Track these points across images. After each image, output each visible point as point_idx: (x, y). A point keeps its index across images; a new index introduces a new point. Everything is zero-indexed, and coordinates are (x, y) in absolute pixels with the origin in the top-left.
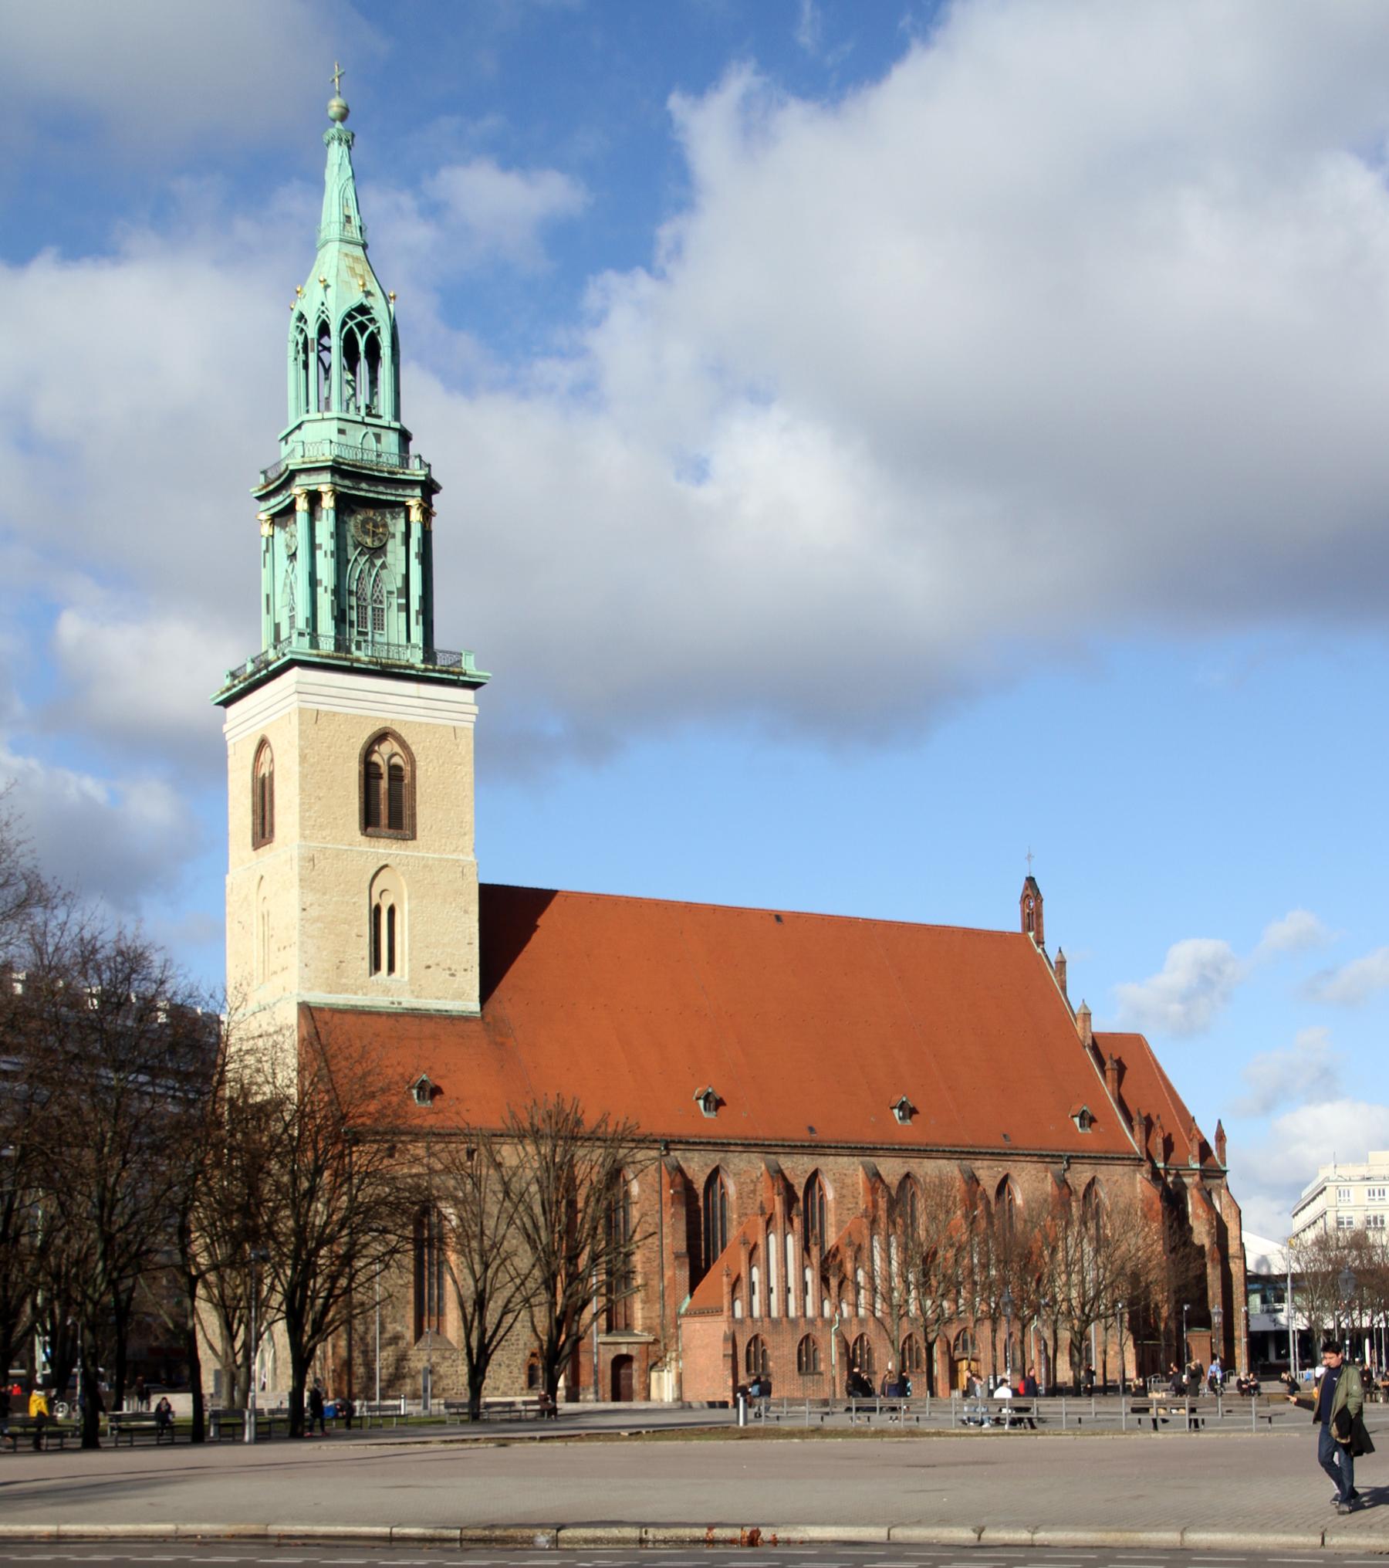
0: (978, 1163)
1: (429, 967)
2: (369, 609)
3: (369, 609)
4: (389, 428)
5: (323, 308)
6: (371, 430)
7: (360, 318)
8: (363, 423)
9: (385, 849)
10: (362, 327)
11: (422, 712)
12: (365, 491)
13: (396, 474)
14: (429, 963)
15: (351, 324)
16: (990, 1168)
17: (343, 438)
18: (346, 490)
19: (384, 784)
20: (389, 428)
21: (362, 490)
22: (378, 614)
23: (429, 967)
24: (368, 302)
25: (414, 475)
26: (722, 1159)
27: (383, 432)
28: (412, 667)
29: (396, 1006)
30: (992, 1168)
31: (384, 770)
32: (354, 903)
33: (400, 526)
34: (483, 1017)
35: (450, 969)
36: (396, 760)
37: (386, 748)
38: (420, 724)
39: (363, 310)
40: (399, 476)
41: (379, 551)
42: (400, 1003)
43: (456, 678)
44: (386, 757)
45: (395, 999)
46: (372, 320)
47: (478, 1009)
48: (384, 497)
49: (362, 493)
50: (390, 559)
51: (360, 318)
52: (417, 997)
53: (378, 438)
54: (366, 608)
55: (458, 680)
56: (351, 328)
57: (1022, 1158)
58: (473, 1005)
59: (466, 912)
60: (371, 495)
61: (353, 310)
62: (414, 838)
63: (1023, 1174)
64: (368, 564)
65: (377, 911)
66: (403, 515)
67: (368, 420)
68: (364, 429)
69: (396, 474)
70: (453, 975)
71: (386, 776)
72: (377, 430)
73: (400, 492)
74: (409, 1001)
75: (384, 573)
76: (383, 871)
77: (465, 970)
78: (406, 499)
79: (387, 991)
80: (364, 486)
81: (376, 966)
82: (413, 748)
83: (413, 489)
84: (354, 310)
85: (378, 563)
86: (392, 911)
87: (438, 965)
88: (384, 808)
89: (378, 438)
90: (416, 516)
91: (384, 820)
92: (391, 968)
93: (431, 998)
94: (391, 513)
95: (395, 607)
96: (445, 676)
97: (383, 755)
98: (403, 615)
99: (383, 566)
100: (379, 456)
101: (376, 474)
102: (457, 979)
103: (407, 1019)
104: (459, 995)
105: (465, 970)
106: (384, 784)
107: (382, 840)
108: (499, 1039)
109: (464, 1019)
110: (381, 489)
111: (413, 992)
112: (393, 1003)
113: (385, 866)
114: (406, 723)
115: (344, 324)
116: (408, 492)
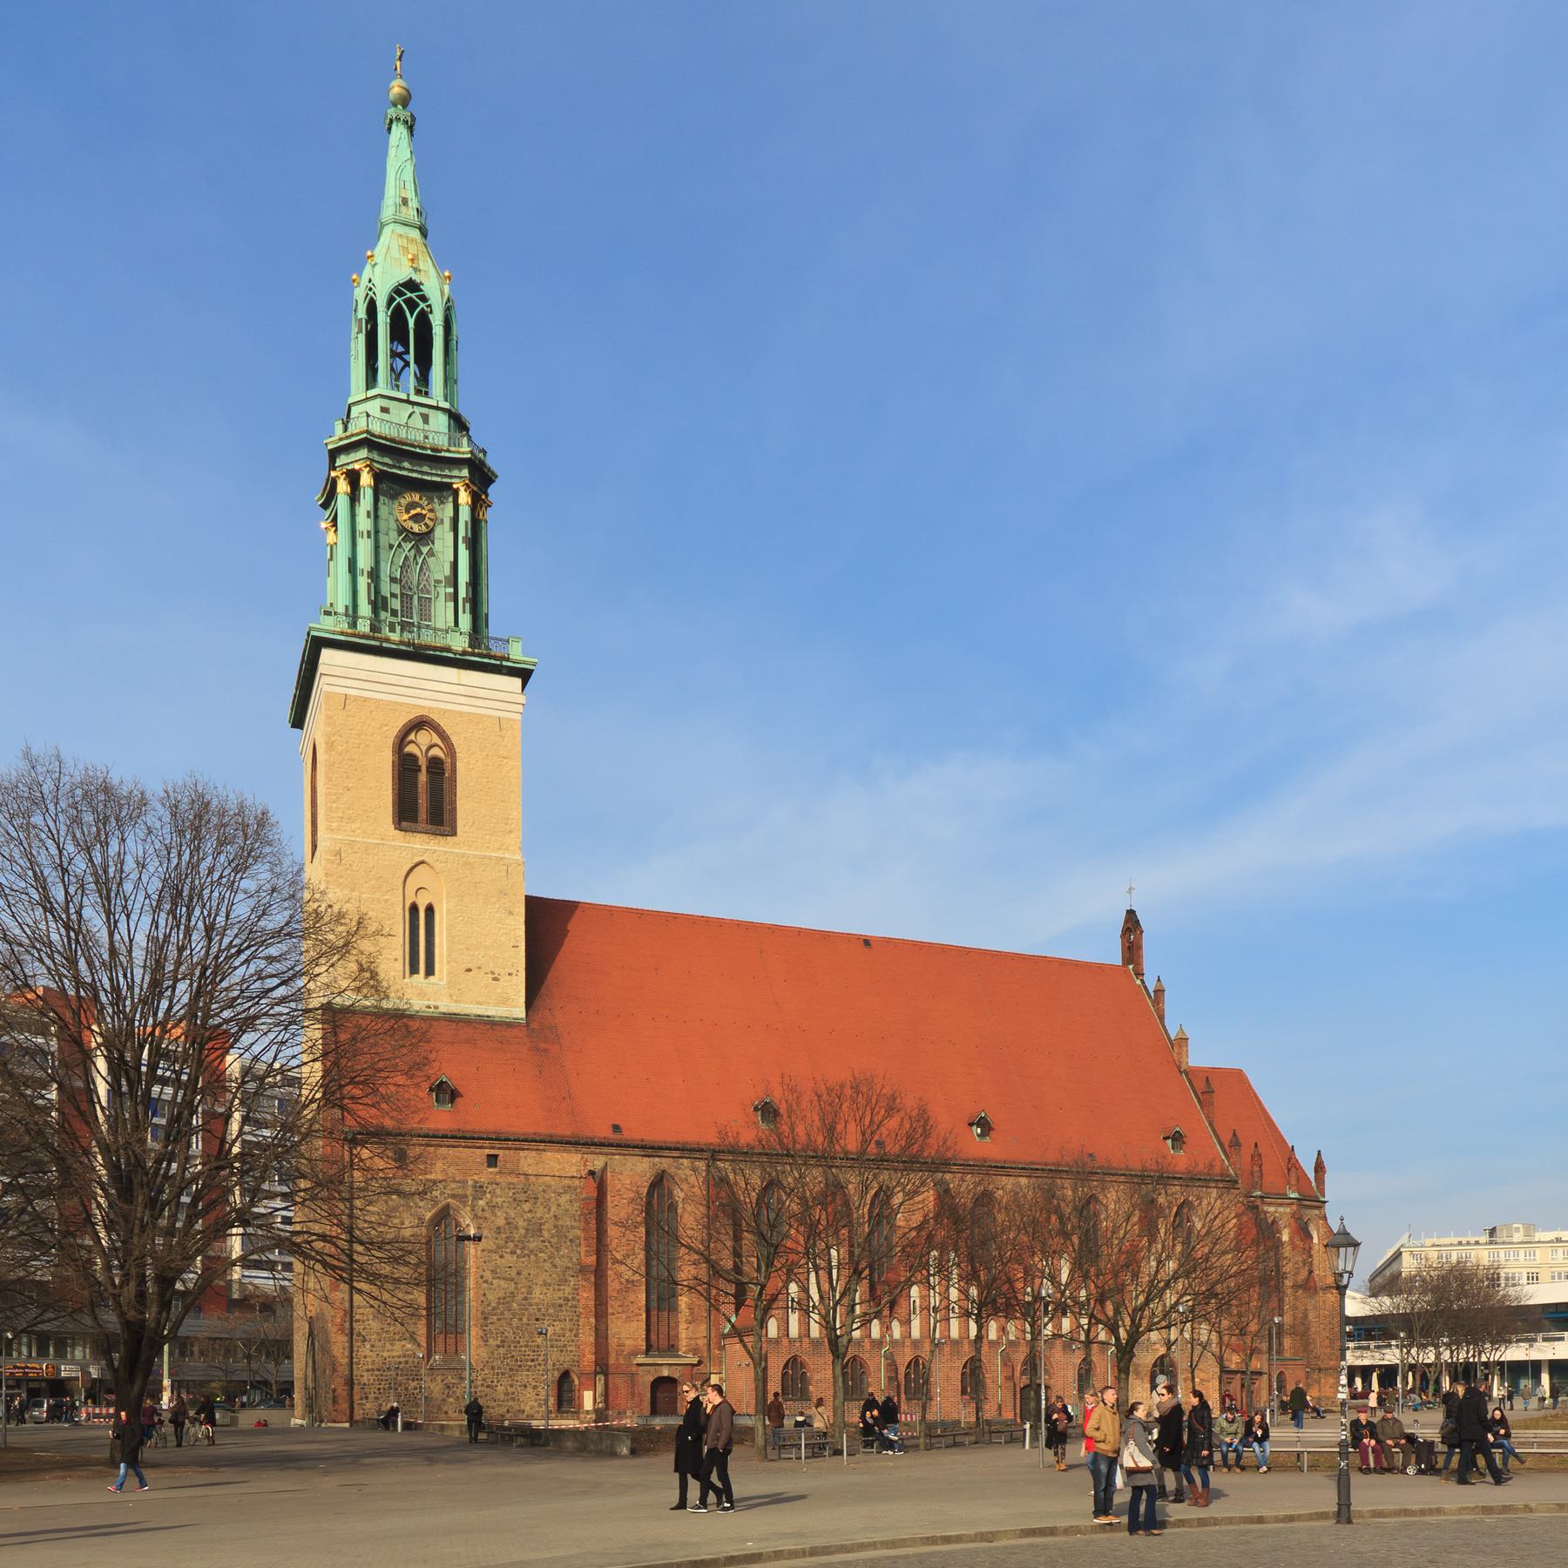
1: (469, 970)
2: (416, 597)
3: (416, 597)
4: (437, 408)
5: (370, 285)
6: (418, 410)
7: (409, 295)
8: (408, 402)
9: (420, 845)
10: (412, 305)
11: (462, 700)
12: (407, 470)
13: (440, 451)
14: (469, 966)
15: (399, 300)
17: (385, 416)
19: (423, 777)
20: (437, 408)
21: (404, 469)
22: (426, 604)
23: (469, 970)
24: (417, 278)
25: (459, 452)
27: (431, 412)
28: (448, 650)
29: (432, 1010)
31: (423, 763)
32: (386, 901)
33: (449, 509)
34: (528, 1024)
35: (493, 973)
36: (435, 752)
37: (424, 738)
38: (461, 714)
39: (412, 285)
40: (443, 454)
41: (426, 537)
42: (436, 1007)
43: (499, 663)
44: (424, 748)
45: (432, 1003)
46: (424, 299)
47: (523, 1015)
48: (429, 478)
49: (405, 473)
50: (438, 546)
51: (409, 295)
52: (456, 1001)
53: (425, 418)
54: (411, 597)
55: (501, 666)
56: (399, 303)
58: (519, 1012)
59: (511, 913)
60: (415, 475)
61: (400, 285)
62: (454, 833)
64: (413, 552)
65: (414, 909)
66: (451, 499)
67: (414, 398)
68: (410, 408)
69: (440, 451)
70: (495, 979)
71: (424, 768)
73: (447, 472)
74: (447, 1005)
75: (431, 560)
76: (422, 865)
77: (510, 974)
78: (453, 481)
79: (422, 994)
80: (406, 465)
81: (414, 970)
82: (454, 739)
83: (460, 470)
84: (403, 285)
85: (425, 550)
86: (430, 910)
87: (479, 968)
88: (423, 801)
89: (425, 418)
90: (464, 498)
91: (423, 814)
92: (430, 971)
93: (471, 1003)
94: (439, 499)
95: (442, 597)
96: (486, 660)
97: (421, 744)
98: (451, 604)
99: (431, 553)
100: (426, 437)
101: (418, 450)
102: (501, 983)
103: (443, 1023)
104: (504, 1001)
105: (510, 974)
106: (423, 777)
107: (419, 835)
108: (542, 1045)
109: (508, 1025)
110: (425, 469)
111: (451, 996)
112: (429, 1007)
113: (423, 862)
114: (446, 711)
115: (391, 300)
116: (455, 473)
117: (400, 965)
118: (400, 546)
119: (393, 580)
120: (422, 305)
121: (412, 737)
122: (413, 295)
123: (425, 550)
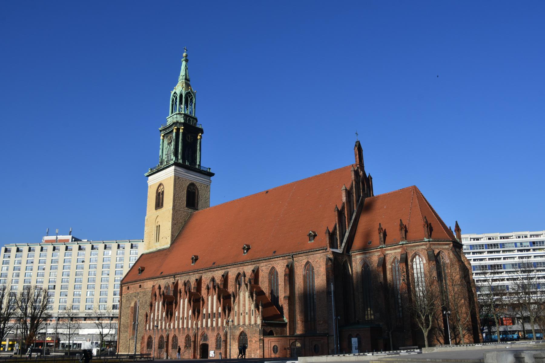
0: (262, 264)
6: (172, 117)
11: (165, 176)
12: (168, 131)
16: (266, 265)
18: (164, 133)
26: (189, 278)
30: (267, 265)
49: (167, 132)
57: (276, 259)
60: (169, 131)
63: (278, 266)
68: (171, 118)
72: (173, 117)
89: (173, 118)
96: (167, 166)
110: (170, 129)
117: (153, 241)
118: (167, 147)
119: (165, 155)
120: (176, 95)
121: (159, 188)
122: (175, 95)
123: (171, 145)
